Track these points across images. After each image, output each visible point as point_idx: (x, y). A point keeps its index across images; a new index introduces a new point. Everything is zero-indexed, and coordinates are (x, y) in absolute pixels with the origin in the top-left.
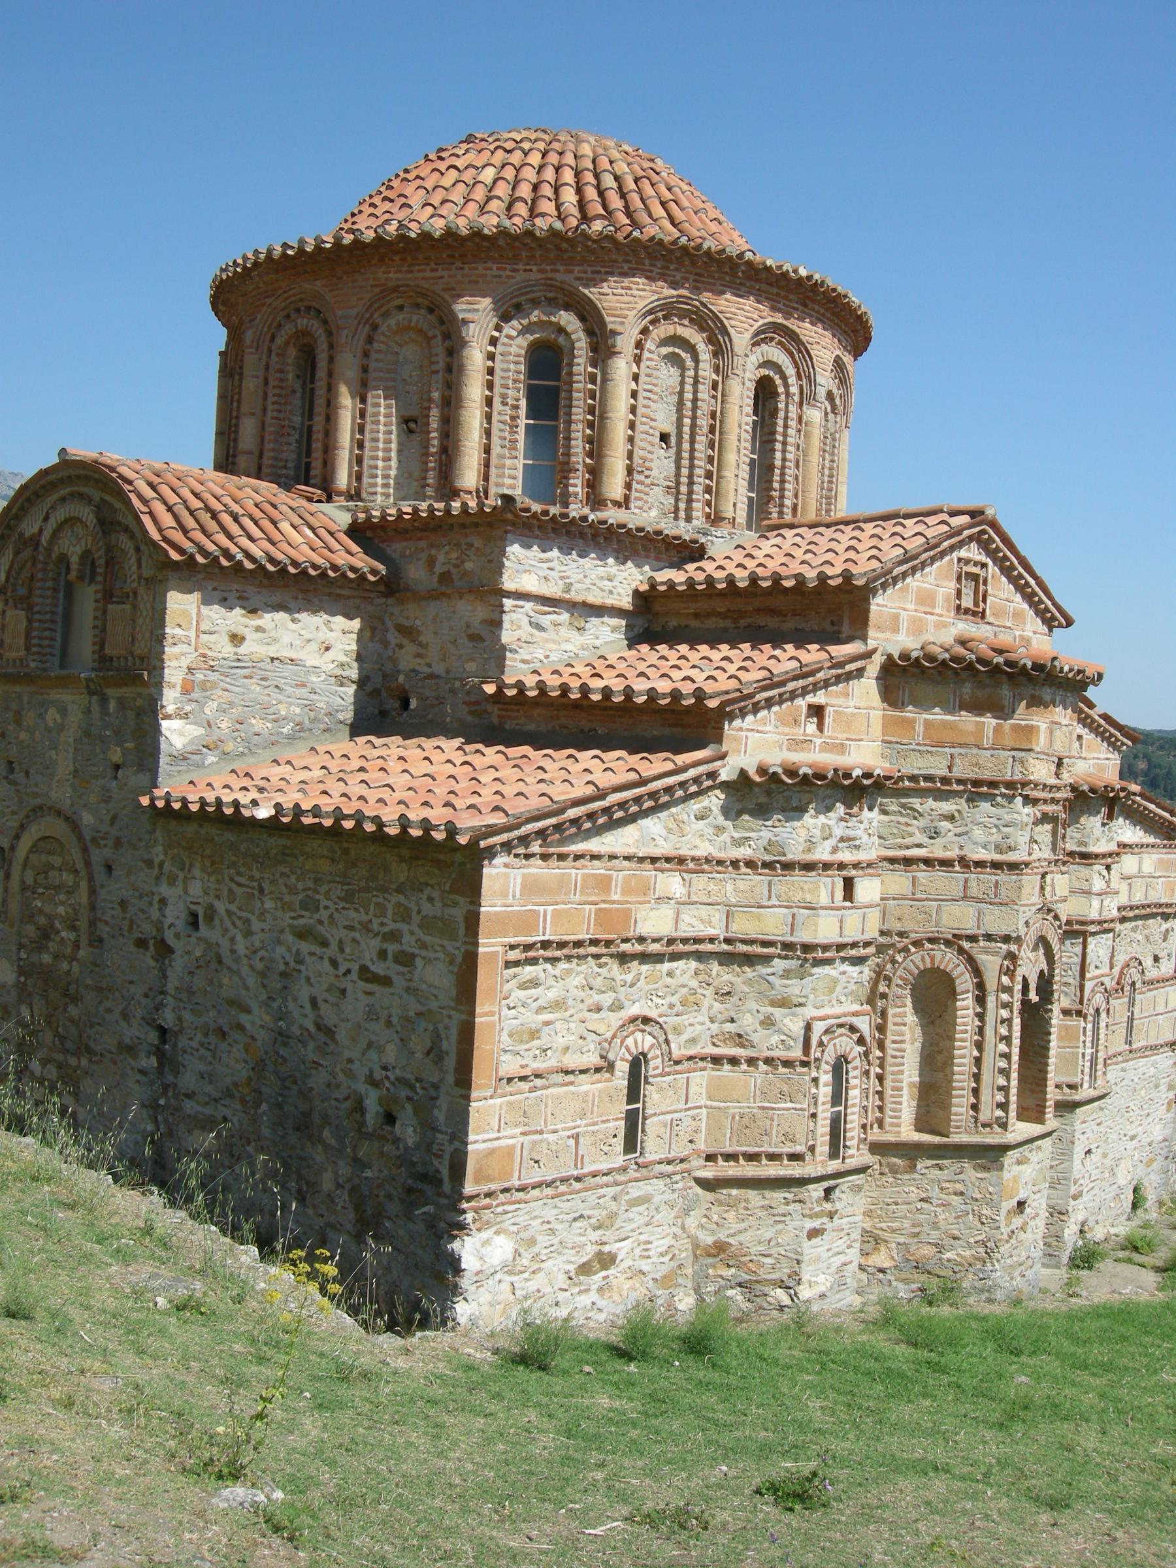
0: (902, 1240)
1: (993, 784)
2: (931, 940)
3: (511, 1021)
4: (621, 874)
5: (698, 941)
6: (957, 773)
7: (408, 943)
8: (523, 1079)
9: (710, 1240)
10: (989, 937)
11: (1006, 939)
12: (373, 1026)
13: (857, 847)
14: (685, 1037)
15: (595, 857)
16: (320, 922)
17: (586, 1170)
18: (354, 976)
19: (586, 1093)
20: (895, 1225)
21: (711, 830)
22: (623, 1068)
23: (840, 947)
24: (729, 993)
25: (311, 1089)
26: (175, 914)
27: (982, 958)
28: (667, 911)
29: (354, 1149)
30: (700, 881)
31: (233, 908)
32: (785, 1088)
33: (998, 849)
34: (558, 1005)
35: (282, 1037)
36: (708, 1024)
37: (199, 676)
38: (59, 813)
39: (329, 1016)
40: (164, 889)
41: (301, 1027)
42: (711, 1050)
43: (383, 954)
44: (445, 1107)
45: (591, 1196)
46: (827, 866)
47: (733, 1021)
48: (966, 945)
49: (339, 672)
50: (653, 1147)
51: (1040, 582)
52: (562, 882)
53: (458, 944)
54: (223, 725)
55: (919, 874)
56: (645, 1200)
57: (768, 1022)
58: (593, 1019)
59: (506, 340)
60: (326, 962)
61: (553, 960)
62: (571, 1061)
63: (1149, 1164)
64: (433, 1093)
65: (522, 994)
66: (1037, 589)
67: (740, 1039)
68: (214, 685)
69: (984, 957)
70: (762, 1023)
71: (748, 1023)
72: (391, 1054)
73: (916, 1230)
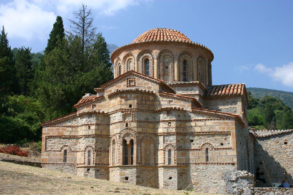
1: (117, 110)
2: (114, 135)
4: (61, 128)
5: (75, 136)
8: (49, 151)
14: (75, 148)
19: (57, 154)
22: (63, 151)
23: (89, 135)
28: (69, 132)
30: (74, 129)
34: (54, 143)
42: (78, 150)
45: (59, 166)
46: (86, 125)
52: (52, 129)
58: (59, 145)
61: (53, 138)
62: (55, 150)
65: (49, 142)
66: (149, 78)
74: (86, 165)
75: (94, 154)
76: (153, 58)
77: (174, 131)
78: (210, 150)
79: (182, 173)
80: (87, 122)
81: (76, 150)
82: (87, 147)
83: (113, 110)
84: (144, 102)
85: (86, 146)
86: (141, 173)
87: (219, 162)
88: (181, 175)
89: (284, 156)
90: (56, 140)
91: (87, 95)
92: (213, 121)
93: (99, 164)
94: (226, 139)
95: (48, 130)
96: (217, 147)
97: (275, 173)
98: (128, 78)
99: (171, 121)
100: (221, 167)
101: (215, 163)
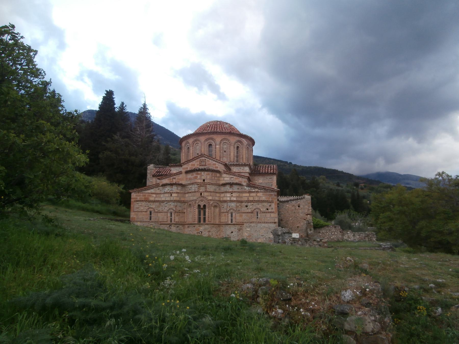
1: (194, 183)
3: (135, 207)
4: (147, 195)
5: (158, 201)
15: (144, 193)
22: (149, 213)
23: (171, 201)
30: (158, 195)
34: (141, 206)
46: (168, 193)
50: (152, 220)
62: (142, 211)
67: (163, 210)
74: (169, 222)
75: (175, 214)
76: (215, 144)
77: (235, 199)
78: (259, 213)
79: (239, 229)
80: (169, 191)
81: (160, 211)
82: (169, 209)
83: (189, 182)
84: (213, 178)
85: (169, 208)
86: (211, 229)
87: (265, 221)
88: (240, 231)
89: (297, 215)
90: (144, 203)
91: (151, 165)
92: (261, 193)
93: (178, 222)
94: (270, 206)
95: (136, 196)
96: (264, 211)
97: (291, 227)
98: (200, 159)
99: (233, 192)
100: (266, 225)
101: (263, 222)
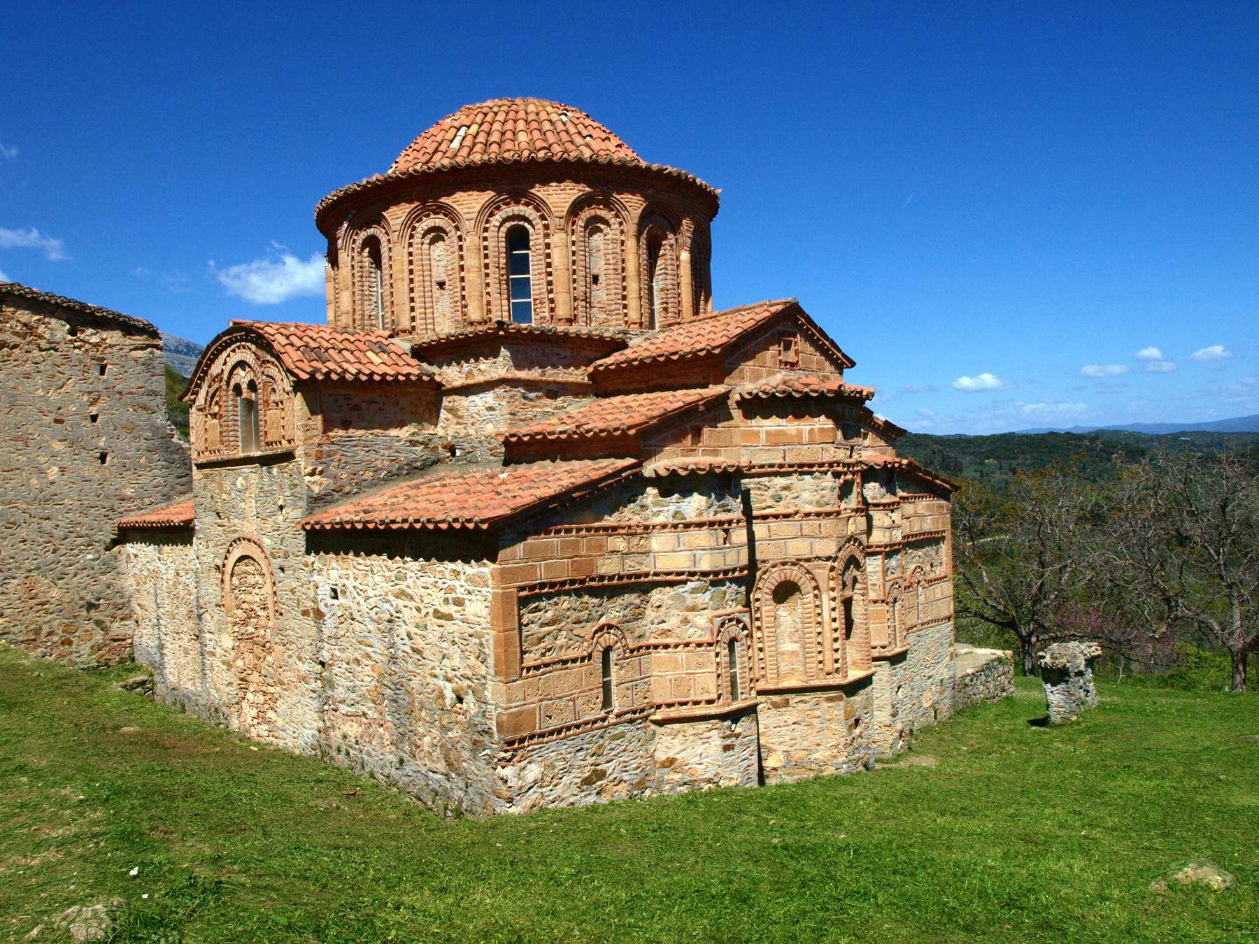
0: (785, 748)
1: (811, 465)
6: (789, 460)
7: (460, 592)
9: (663, 758)
10: (819, 558)
11: (828, 559)
12: (445, 645)
13: (729, 511)
14: (636, 634)
16: (408, 587)
17: (581, 720)
18: (431, 616)
20: (781, 739)
21: (638, 508)
22: (597, 657)
23: (726, 572)
24: (659, 606)
25: (413, 688)
26: (325, 591)
27: (816, 572)
29: (440, 721)
31: (357, 584)
32: (700, 660)
33: (819, 504)
35: (393, 659)
36: (649, 625)
37: (325, 448)
38: (249, 540)
39: (420, 643)
40: (316, 577)
41: (404, 652)
43: (446, 601)
44: (490, 688)
46: (712, 524)
47: (664, 622)
48: (806, 565)
49: (410, 438)
51: (832, 343)
53: (489, 589)
54: (343, 477)
55: (771, 524)
56: (622, 735)
57: (686, 621)
59: (493, 229)
60: (414, 610)
63: (942, 693)
64: (483, 681)
68: (335, 452)
69: (817, 571)
70: (682, 622)
71: (673, 622)
72: (456, 661)
73: (794, 742)
81: (643, 642)
